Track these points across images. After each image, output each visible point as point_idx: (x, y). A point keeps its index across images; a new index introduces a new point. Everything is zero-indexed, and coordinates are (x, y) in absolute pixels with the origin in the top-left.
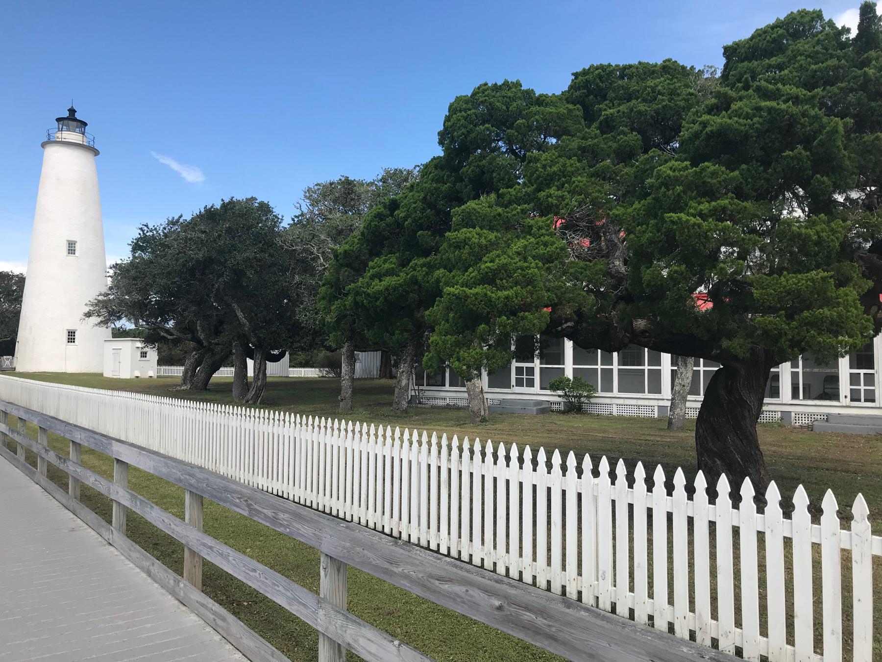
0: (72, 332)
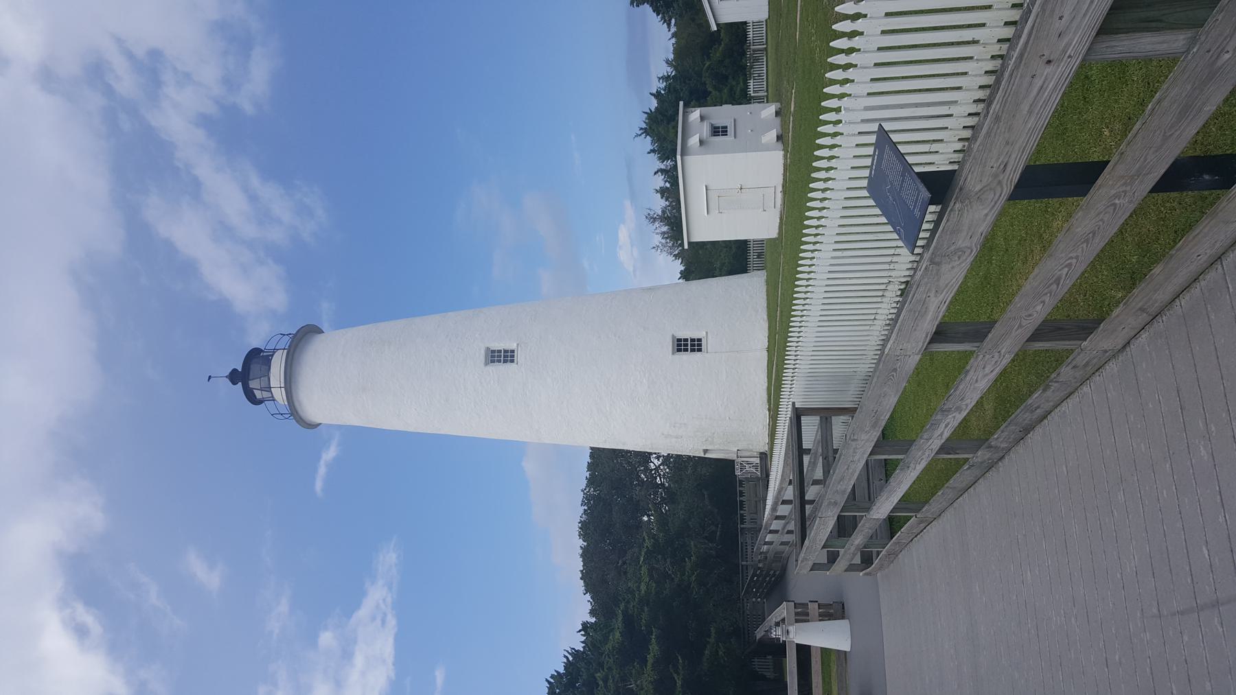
0: (678, 345)
